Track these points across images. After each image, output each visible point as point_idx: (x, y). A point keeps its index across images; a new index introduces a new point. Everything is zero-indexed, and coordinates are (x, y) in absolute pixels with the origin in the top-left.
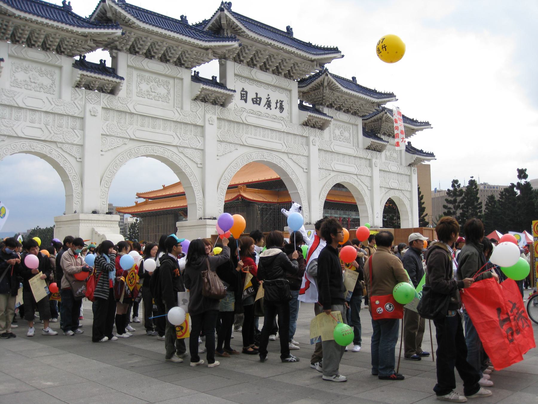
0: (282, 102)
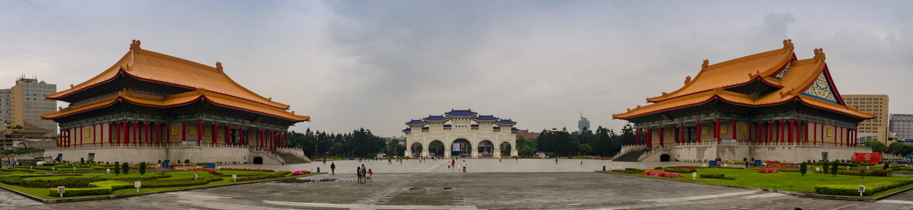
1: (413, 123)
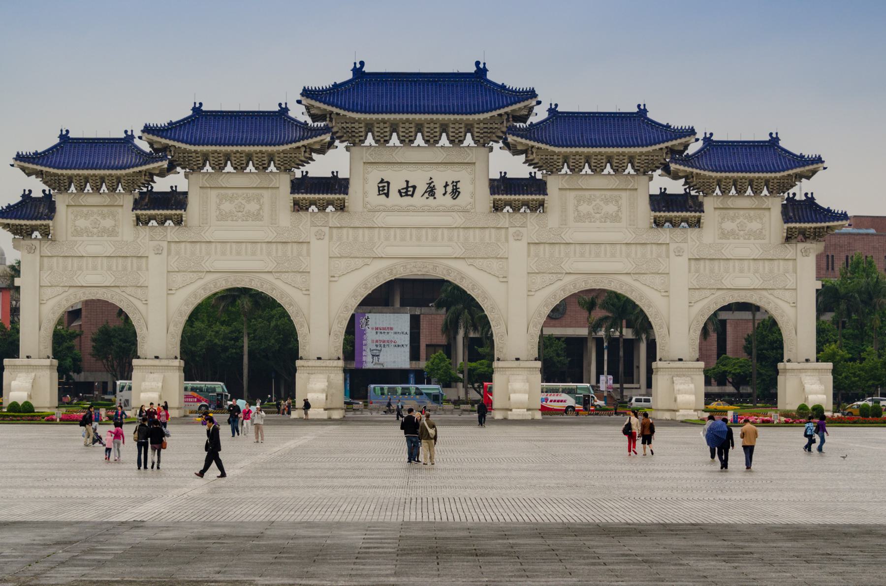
0: (455, 184)
1: (72, 160)
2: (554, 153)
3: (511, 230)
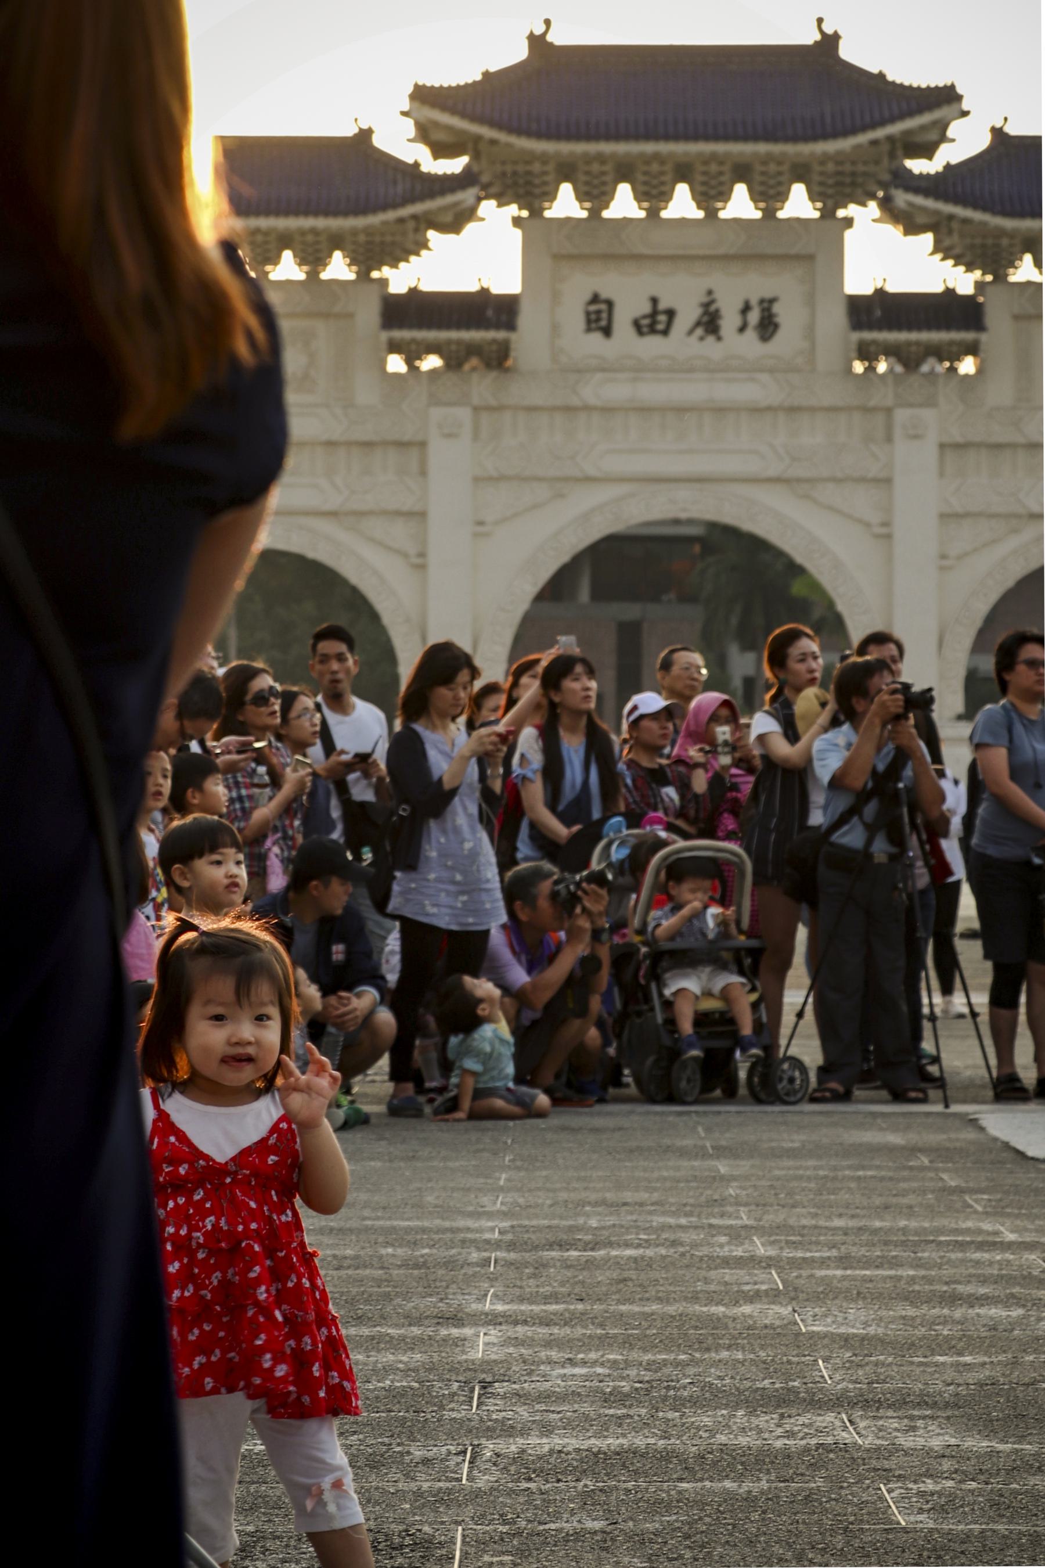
0: (767, 305)
2: (1001, 232)
3: (901, 415)
